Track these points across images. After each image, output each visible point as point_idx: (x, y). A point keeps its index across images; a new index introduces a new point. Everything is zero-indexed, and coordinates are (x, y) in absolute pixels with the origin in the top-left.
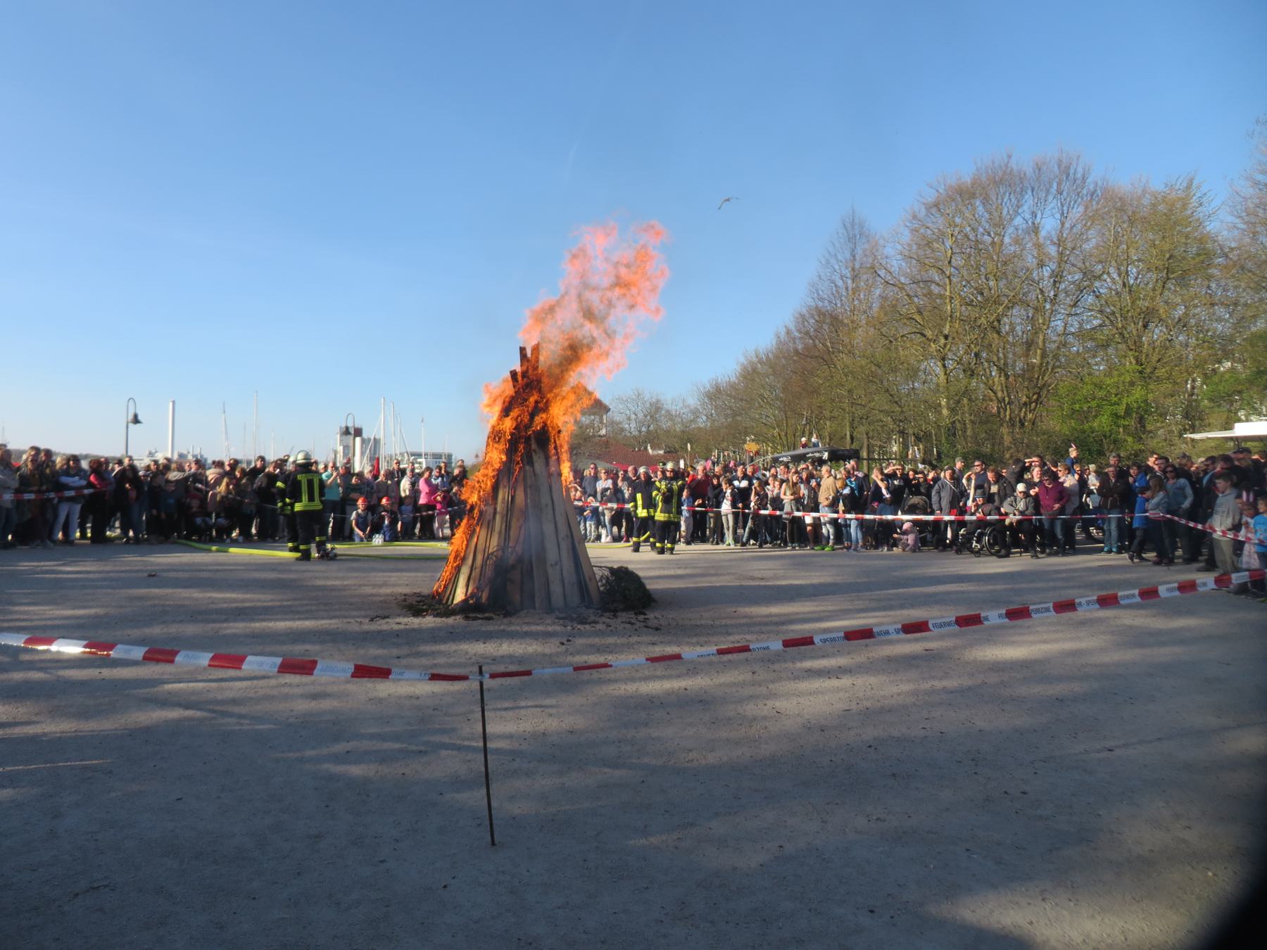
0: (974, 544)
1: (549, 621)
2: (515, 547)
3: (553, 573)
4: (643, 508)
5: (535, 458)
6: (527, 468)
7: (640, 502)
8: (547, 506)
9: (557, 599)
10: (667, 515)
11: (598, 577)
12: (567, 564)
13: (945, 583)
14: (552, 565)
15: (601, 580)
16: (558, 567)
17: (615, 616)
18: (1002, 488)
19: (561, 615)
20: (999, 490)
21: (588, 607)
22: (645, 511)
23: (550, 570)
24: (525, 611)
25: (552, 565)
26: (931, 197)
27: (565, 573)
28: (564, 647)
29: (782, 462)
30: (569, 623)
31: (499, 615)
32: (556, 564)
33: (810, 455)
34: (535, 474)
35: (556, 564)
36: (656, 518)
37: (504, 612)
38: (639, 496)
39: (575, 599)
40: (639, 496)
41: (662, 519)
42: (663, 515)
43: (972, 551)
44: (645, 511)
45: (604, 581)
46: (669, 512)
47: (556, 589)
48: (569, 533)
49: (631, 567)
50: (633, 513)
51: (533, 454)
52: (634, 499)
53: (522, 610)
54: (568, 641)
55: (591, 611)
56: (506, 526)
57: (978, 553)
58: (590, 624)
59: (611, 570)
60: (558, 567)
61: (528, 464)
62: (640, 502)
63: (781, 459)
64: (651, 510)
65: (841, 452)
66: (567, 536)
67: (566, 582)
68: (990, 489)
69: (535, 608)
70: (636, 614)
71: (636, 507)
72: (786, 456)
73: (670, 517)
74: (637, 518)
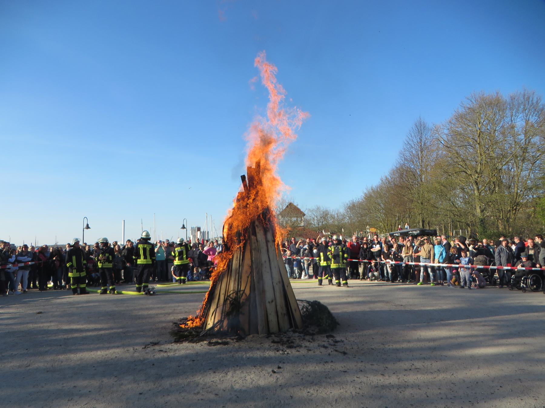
0: (522, 284)
1: (266, 345)
2: (244, 291)
3: (271, 308)
4: (324, 261)
5: (257, 230)
6: (253, 237)
7: (322, 258)
8: (265, 262)
9: (273, 326)
10: (337, 264)
11: (300, 307)
12: (280, 301)
13: (522, 312)
14: (269, 302)
15: (303, 309)
16: (274, 303)
17: (314, 340)
18: (537, 252)
19: (276, 339)
20: (535, 253)
21: (294, 332)
22: (325, 262)
23: (268, 305)
24: (251, 336)
25: (269, 302)
26: (468, 104)
27: (278, 307)
28: (275, 375)
29: (411, 234)
30: (281, 347)
31: (233, 340)
32: (272, 301)
33: (411, 232)
34: (257, 241)
35: (272, 301)
36: (331, 267)
37: (236, 337)
38: (322, 254)
39: (285, 325)
40: (322, 254)
41: (335, 267)
42: (335, 265)
43: (520, 289)
44: (325, 262)
45: (305, 310)
46: (338, 263)
47: (272, 318)
48: (281, 280)
49: (322, 301)
50: (318, 264)
51: (256, 227)
52: (319, 256)
53: (249, 335)
54: (279, 368)
55: (297, 334)
56: (239, 276)
57: (524, 290)
58: (295, 348)
59: (308, 302)
60: (274, 303)
61: (253, 234)
62: (322, 258)
63: (395, 235)
64: (329, 262)
65: (427, 231)
66: (279, 282)
67: (279, 314)
68: (529, 252)
69: (258, 333)
70: (327, 337)
71: (320, 260)
72: (397, 233)
73: (339, 266)
74: (320, 266)
